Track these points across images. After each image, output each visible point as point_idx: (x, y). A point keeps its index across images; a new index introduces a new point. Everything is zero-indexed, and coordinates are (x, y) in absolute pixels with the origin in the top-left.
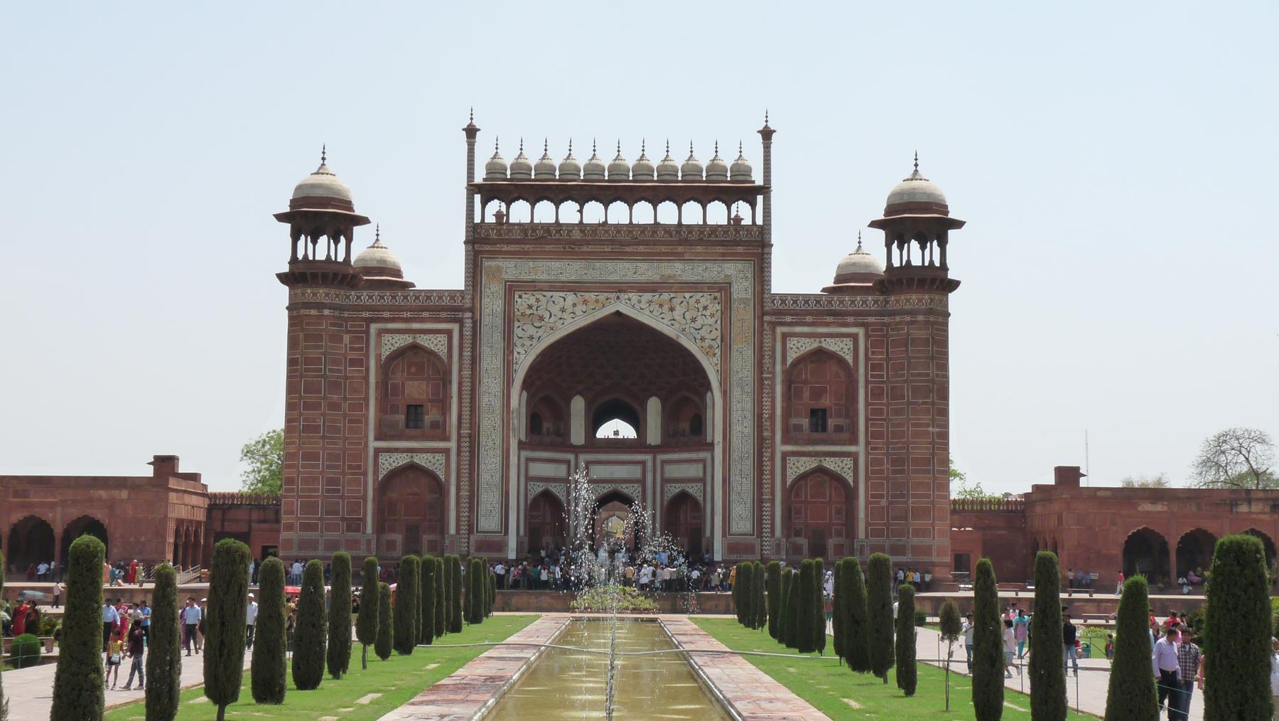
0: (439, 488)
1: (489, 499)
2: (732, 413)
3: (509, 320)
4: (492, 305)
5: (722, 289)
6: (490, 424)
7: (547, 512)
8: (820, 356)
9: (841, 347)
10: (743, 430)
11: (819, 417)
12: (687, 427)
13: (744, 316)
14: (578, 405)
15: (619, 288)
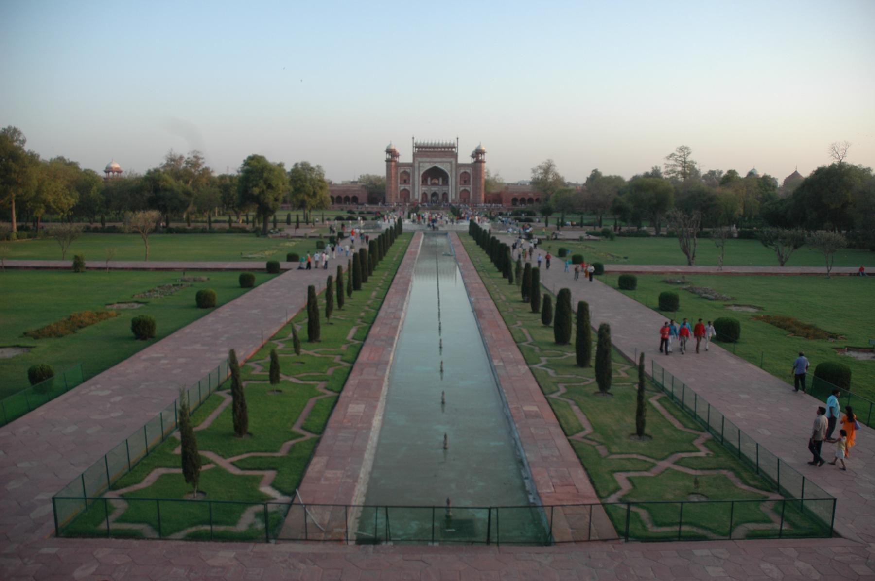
0: (409, 192)
1: (416, 194)
2: (452, 181)
3: (419, 167)
4: (416, 165)
5: (451, 162)
6: (416, 182)
7: (425, 195)
8: (465, 173)
9: (468, 171)
10: (454, 183)
11: (465, 181)
12: (446, 182)
13: (454, 166)
14: (429, 179)
15: (435, 162)
